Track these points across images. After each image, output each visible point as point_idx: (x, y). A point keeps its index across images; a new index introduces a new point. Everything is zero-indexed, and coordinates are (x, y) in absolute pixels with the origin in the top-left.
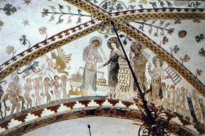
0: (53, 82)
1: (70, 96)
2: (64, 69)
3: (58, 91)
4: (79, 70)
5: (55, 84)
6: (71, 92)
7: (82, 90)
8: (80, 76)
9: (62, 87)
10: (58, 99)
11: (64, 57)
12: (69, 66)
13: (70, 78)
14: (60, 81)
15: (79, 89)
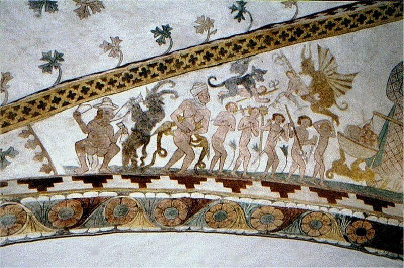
0: (294, 128)
1: (332, 175)
2: (329, 106)
3: (301, 153)
4: (372, 118)
5: (298, 134)
6: (338, 166)
7: (372, 170)
8: (372, 133)
9: (314, 148)
10: (297, 172)
11: (335, 76)
12: (343, 103)
13: (342, 131)
14: (312, 131)
15: (362, 166)
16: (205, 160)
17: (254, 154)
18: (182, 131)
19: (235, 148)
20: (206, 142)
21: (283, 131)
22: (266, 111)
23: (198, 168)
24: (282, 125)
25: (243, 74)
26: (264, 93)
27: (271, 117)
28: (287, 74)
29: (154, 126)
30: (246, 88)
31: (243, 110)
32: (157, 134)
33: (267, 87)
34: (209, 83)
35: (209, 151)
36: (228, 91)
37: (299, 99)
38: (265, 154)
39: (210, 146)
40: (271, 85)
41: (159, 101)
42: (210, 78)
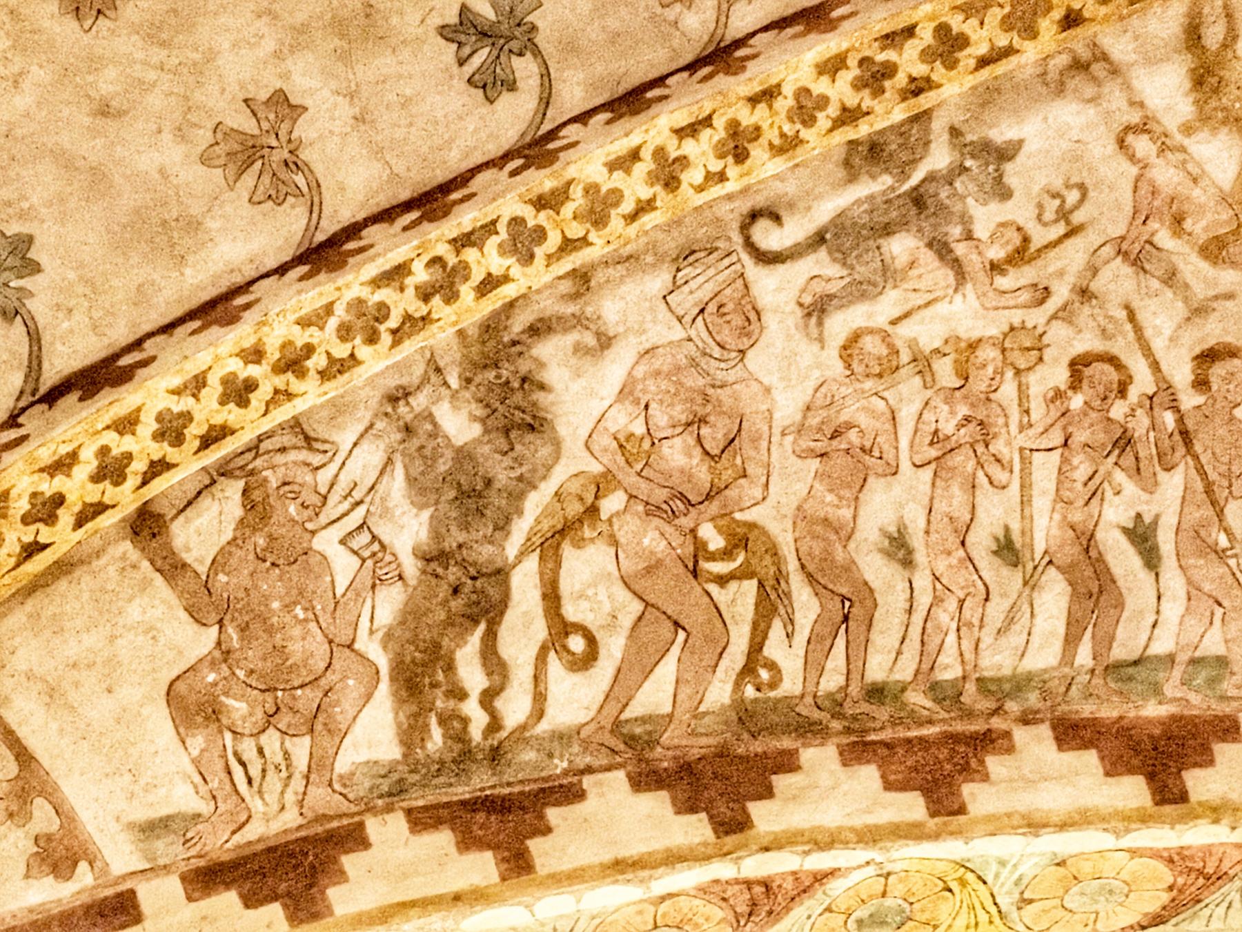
16: (774, 648)
17: (1006, 581)
18: (653, 510)
19: (908, 562)
20: (773, 551)
21: (1124, 442)
22: (1038, 348)
23: (750, 692)
24: (1118, 410)
25: (904, 175)
26: (1021, 254)
27: (1060, 376)
28: (1121, 143)
29: (520, 512)
30: (930, 245)
31: (923, 363)
32: (535, 556)
33: (1033, 229)
34: (749, 245)
35: (788, 595)
36: (845, 272)
37: (1194, 268)
38: (1052, 571)
39: (792, 565)
40: (1049, 215)
41: (524, 380)
42: (754, 216)
